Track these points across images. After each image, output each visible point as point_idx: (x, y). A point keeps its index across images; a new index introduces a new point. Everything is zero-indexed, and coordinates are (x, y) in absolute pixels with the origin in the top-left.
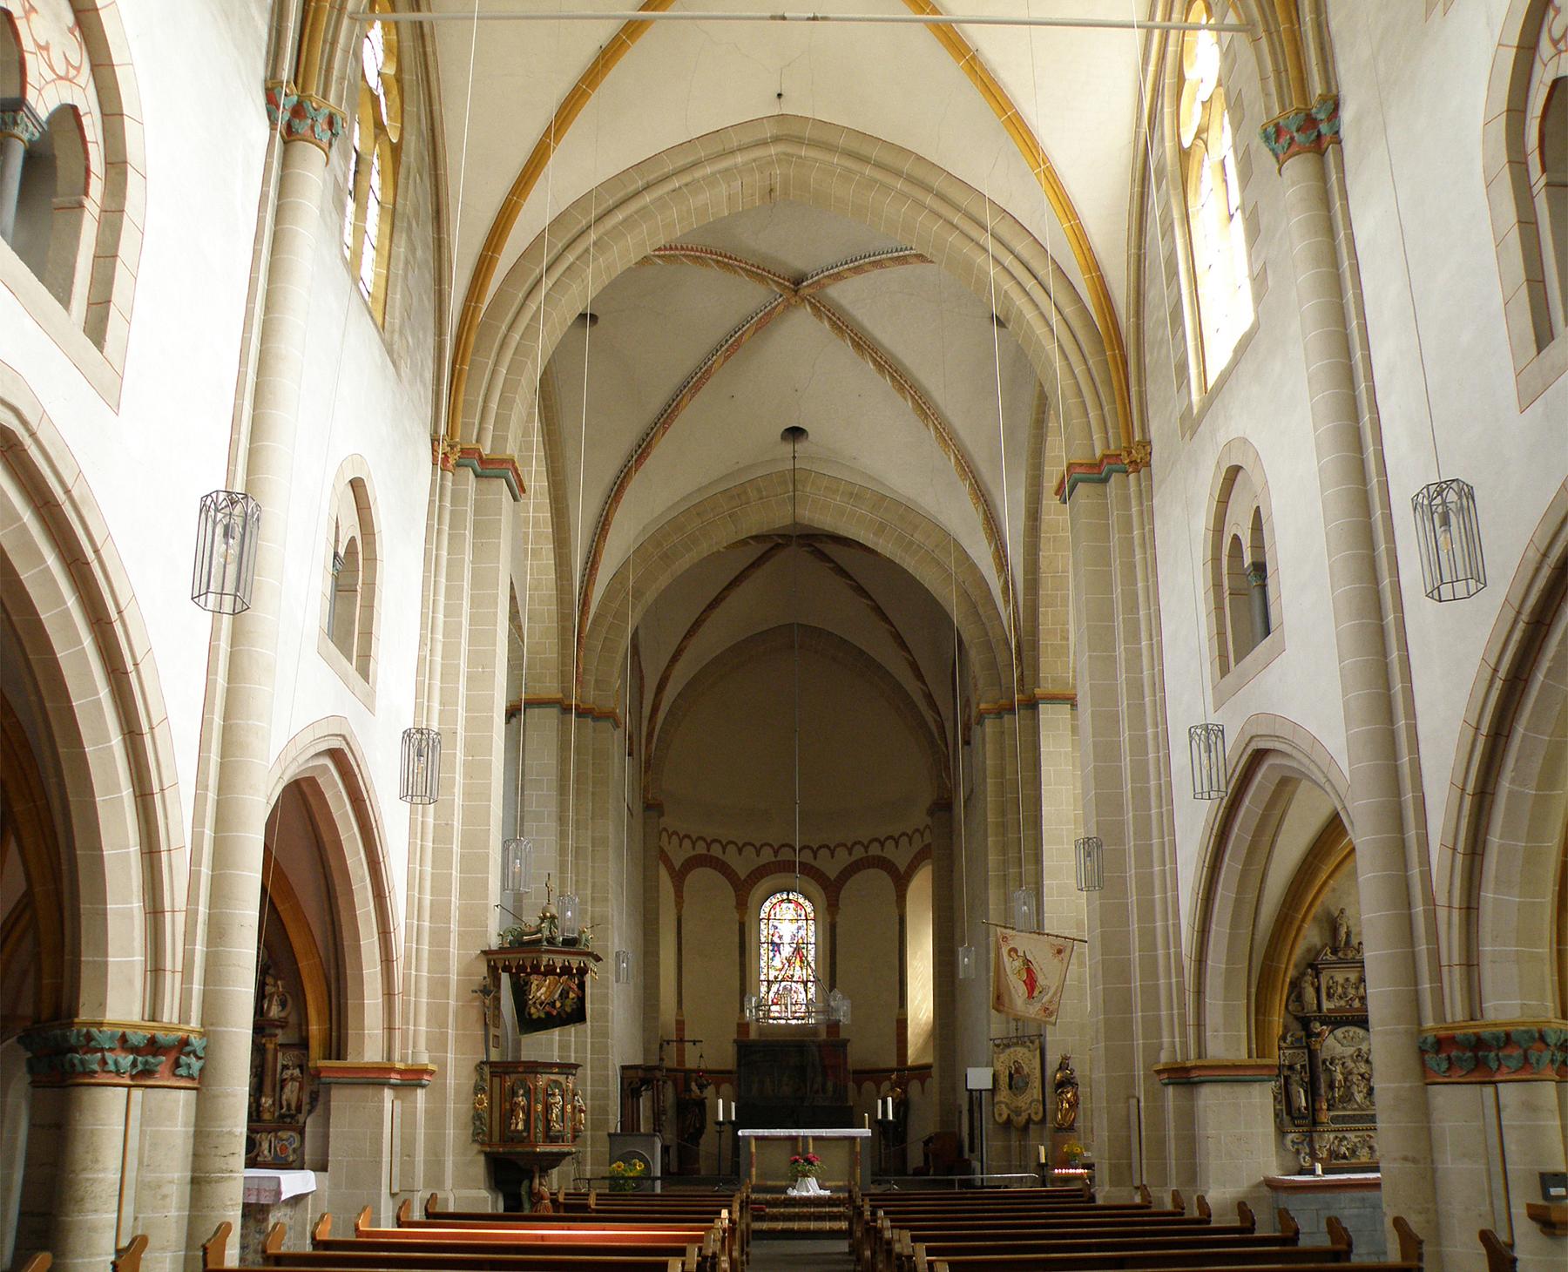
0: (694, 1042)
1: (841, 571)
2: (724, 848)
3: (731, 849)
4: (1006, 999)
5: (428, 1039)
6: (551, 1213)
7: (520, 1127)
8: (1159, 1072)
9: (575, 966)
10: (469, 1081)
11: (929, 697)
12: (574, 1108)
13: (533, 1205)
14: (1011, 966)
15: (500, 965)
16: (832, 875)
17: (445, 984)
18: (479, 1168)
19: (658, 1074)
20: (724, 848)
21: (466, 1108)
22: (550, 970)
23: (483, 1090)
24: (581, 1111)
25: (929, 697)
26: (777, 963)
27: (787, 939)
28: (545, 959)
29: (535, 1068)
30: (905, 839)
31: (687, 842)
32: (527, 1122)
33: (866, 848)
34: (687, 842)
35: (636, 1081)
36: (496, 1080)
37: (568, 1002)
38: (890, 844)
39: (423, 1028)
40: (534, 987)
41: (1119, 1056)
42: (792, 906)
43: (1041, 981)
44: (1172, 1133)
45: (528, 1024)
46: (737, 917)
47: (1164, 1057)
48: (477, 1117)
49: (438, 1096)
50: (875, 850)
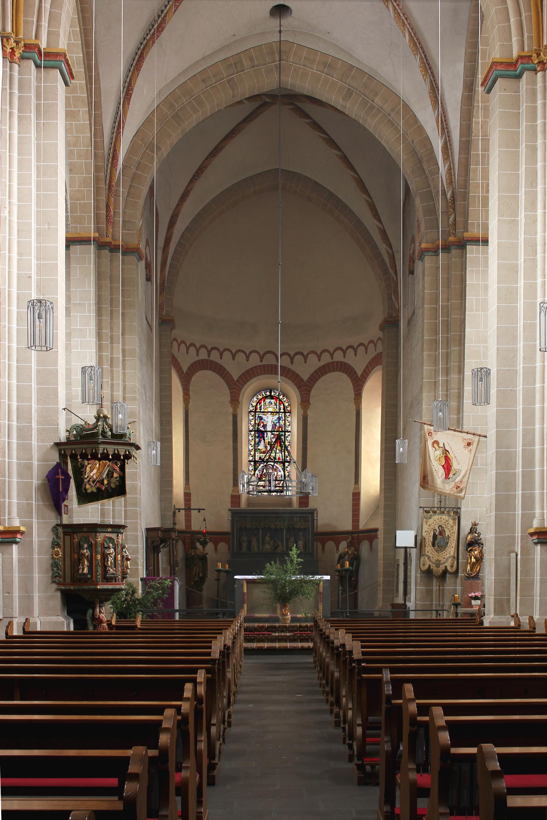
0: (199, 510)
1: (316, 126)
2: (221, 355)
3: (227, 355)
4: (429, 478)
5: (18, 509)
6: (107, 630)
7: (86, 571)
8: (532, 534)
9: (122, 453)
10: (48, 538)
11: (383, 233)
12: (123, 557)
13: (95, 627)
14: (434, 455)
15: (68, 453)
16: (305, 377)
17: (29, 467)
18: (57, 600)
19: (174, 535)
20: (221, 355)
21: (47, 557)
22: (105, 457)
23: (58, 545)
24: (128, 559)
25: (383, 233)
26: (261, 447)
27: (269, 428)
28: (101, 449)
29: (93, 528)
30: (362, 348)
31: (192, 350)
32: (90, 567)
33: (332, 355)
34: (192, 349)
35: (156, 540)
36: (68, 538)
37: (113, 480)
38: (351, 352)
39: (15, 501)
40: (88, 469)
41: (503, 523)
42: (273, 401)
43: (455, 465)
44: (538, 578)
45: (85, 498)
46: (231, 410)
47: (536, 524)
48: (54, 564)
49: (27, 549)
50: (338, 357)
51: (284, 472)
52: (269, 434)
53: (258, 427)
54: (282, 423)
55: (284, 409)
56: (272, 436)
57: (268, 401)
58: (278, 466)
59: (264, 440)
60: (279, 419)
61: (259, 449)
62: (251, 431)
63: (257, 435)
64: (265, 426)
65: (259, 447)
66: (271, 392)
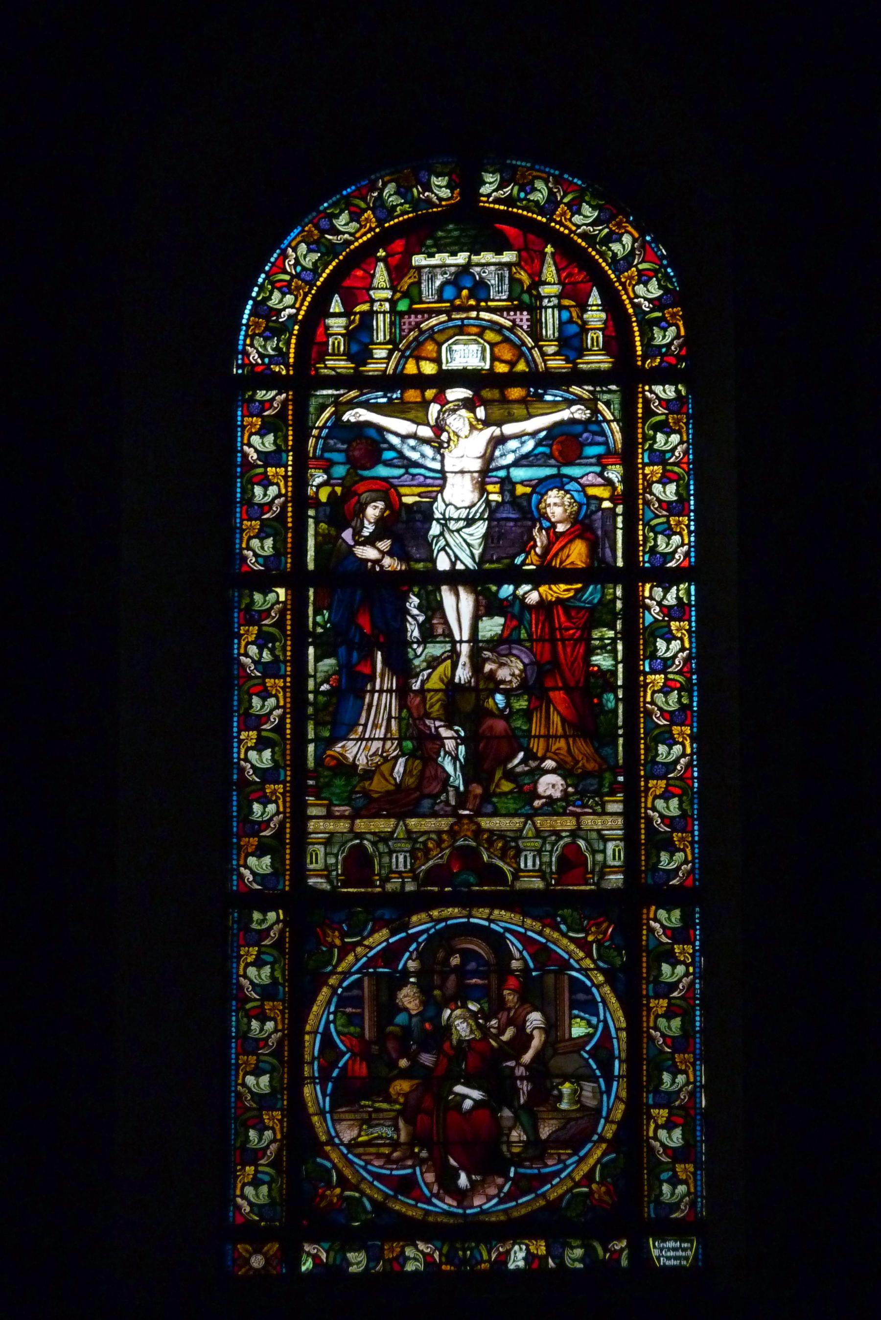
27: (460, 546)
51: (634, 1009)
52: (458, 606)
53: (326, 544)
54: (600, 482)
55: (617, 338)
56: (492, 626)
57: (437, 263)
58: (564, 946)
59: (402, 668)
60: (564, 444)
61: (347, 769)
62: (264, 582)
63: (317, 620)
64: (409, 526)
65: (351, 750)
66: (467, 185)
